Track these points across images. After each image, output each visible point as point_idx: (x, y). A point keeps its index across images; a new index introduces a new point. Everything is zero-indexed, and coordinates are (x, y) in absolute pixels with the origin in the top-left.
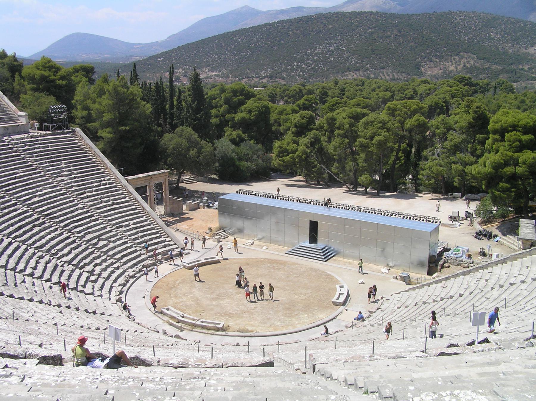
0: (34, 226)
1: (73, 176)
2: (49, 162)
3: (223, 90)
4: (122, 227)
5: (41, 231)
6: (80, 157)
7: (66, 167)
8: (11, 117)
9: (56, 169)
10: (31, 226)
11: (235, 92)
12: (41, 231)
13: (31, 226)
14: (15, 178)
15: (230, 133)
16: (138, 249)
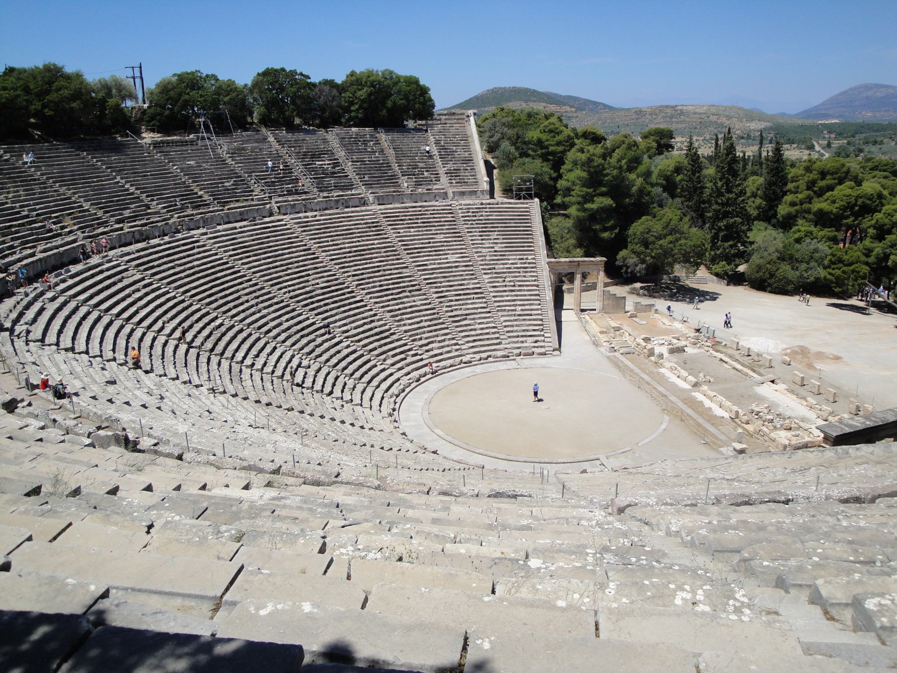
0: (405, 291)
1: (496, 249)
2: (480, 232)
3: (808, 169)
4: (505, 310)
5: (407, 297)
6: (520, 231)
7: (495, 239)
8: (476, 182)
9: (482, 240)
10: (400, 290)
11: (823, 174)
12: (407, 297)
13: (400, 290)
14: (430, 243)
15: (802, 226)
16: (502, 337)
